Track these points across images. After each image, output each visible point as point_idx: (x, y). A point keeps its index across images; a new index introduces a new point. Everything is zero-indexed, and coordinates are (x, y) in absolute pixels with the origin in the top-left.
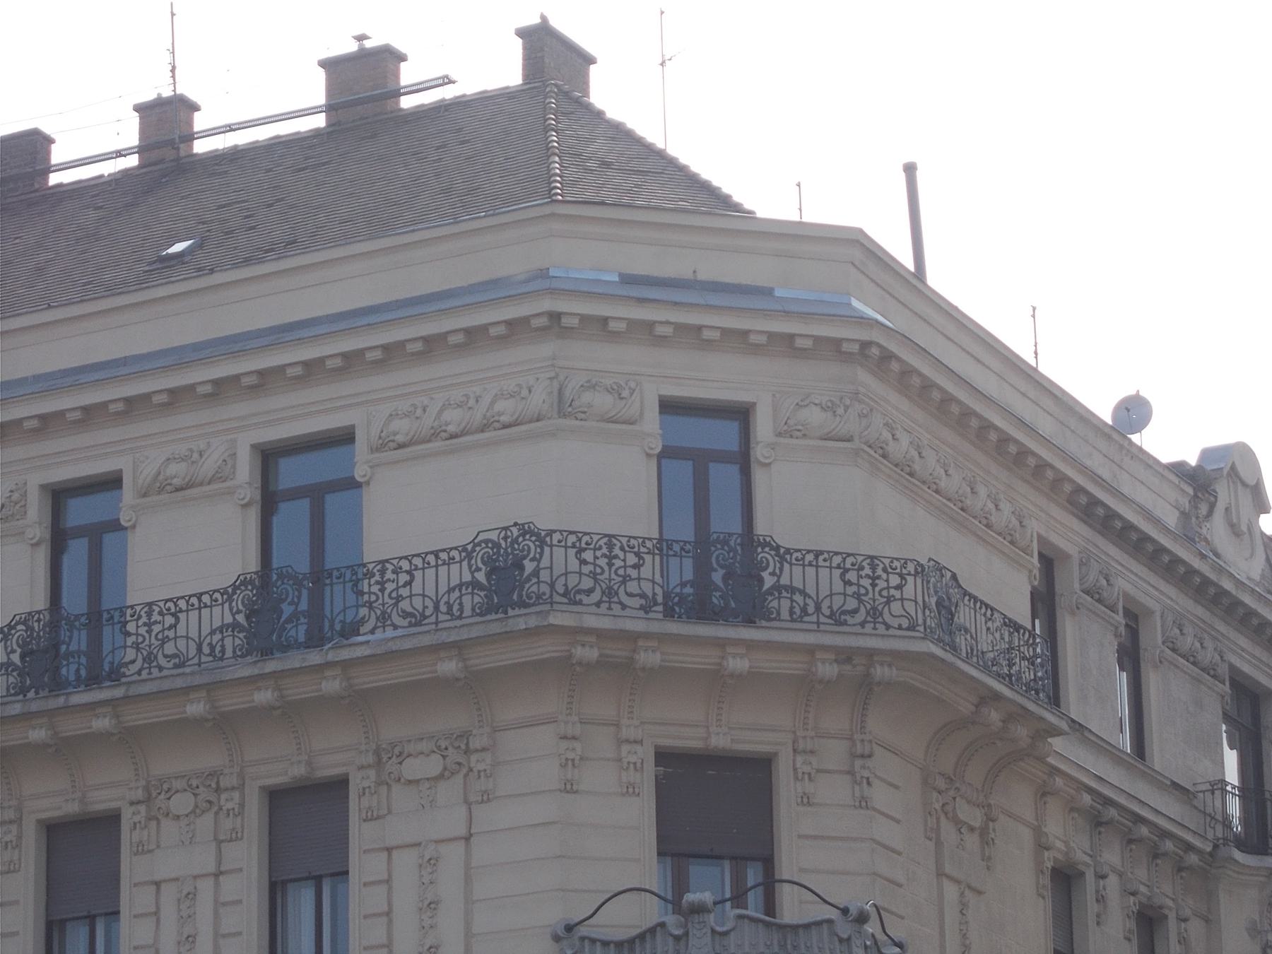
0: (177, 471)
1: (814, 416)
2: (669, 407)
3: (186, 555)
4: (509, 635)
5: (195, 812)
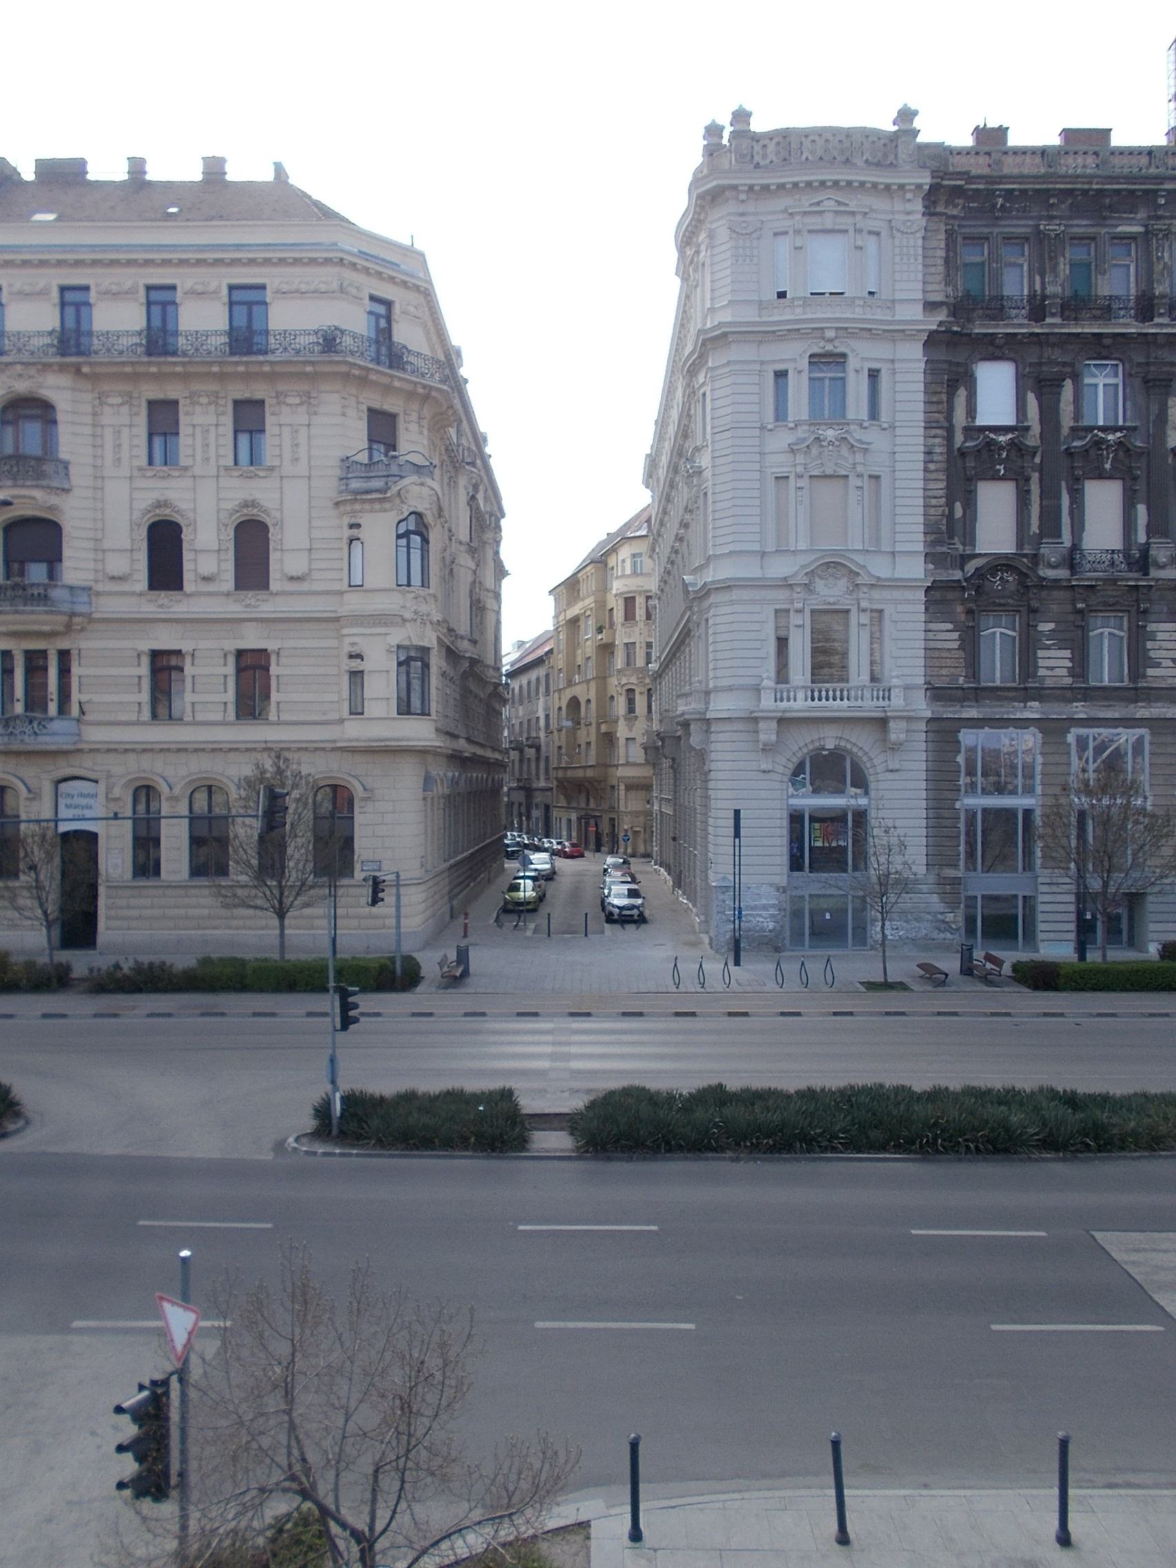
0: (200, 288)
1: (412, 309)
2: (373, 298)
3: (202, 319)
4: (331, 362)
5: (210, 404)
